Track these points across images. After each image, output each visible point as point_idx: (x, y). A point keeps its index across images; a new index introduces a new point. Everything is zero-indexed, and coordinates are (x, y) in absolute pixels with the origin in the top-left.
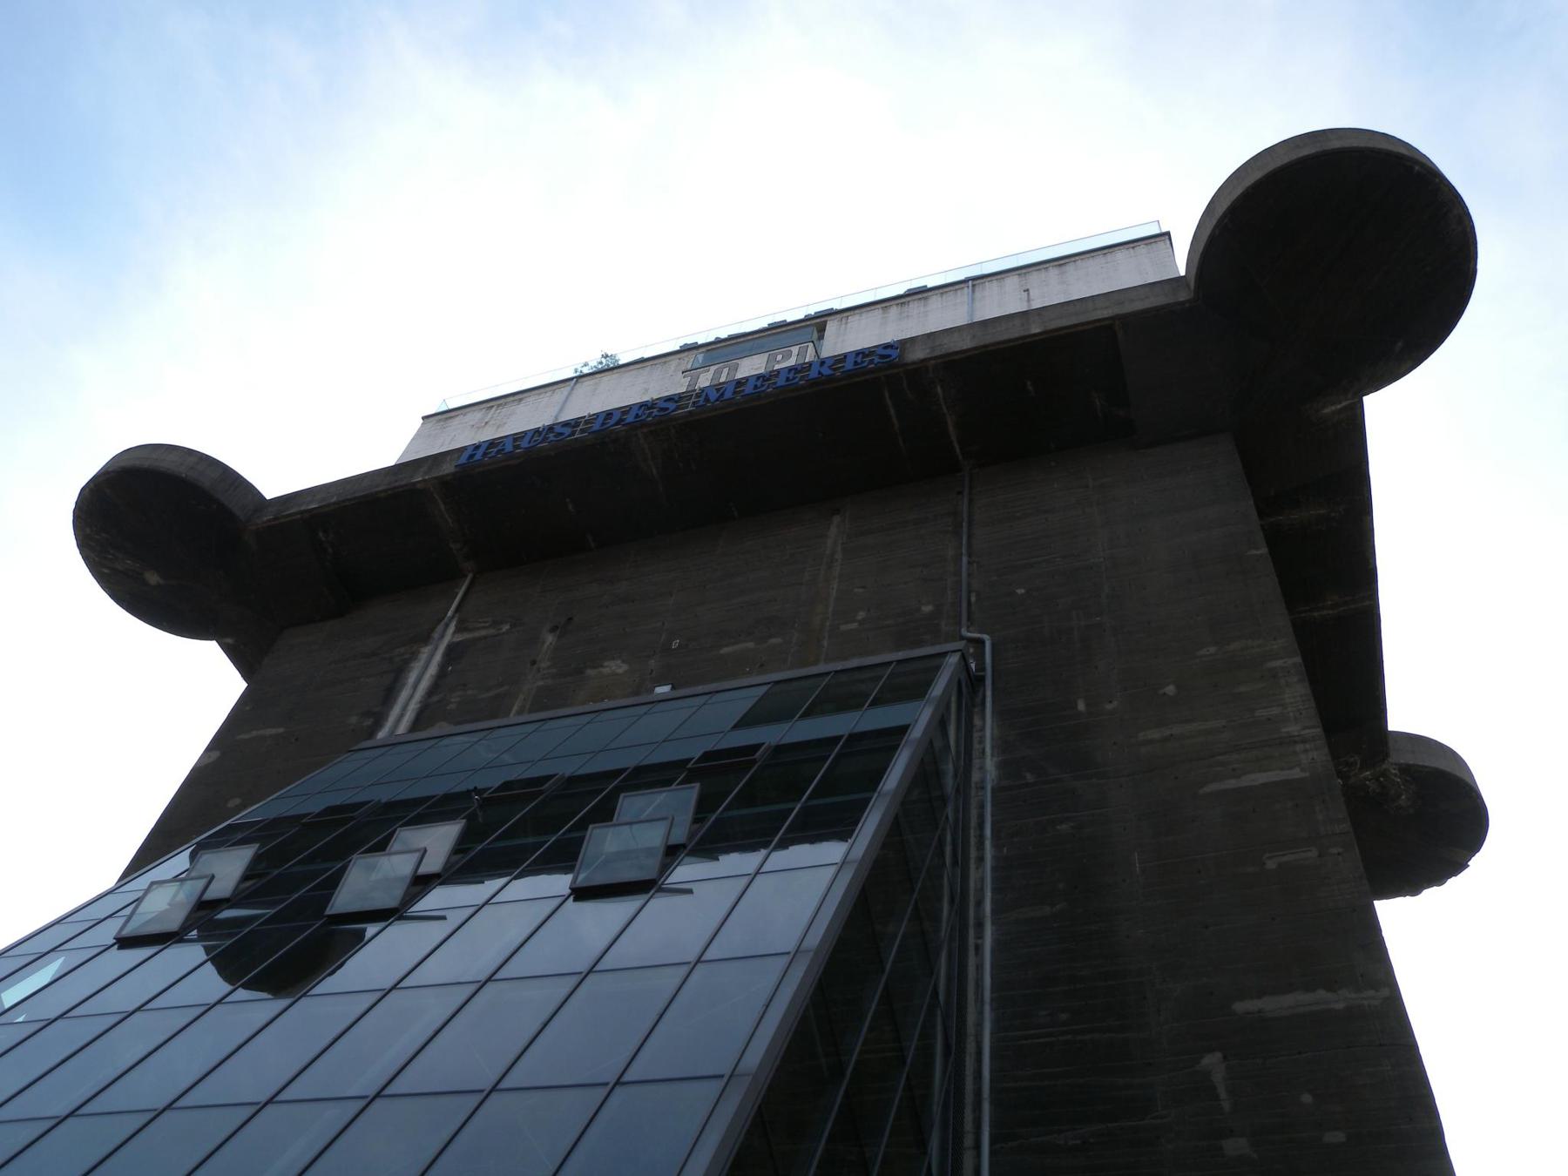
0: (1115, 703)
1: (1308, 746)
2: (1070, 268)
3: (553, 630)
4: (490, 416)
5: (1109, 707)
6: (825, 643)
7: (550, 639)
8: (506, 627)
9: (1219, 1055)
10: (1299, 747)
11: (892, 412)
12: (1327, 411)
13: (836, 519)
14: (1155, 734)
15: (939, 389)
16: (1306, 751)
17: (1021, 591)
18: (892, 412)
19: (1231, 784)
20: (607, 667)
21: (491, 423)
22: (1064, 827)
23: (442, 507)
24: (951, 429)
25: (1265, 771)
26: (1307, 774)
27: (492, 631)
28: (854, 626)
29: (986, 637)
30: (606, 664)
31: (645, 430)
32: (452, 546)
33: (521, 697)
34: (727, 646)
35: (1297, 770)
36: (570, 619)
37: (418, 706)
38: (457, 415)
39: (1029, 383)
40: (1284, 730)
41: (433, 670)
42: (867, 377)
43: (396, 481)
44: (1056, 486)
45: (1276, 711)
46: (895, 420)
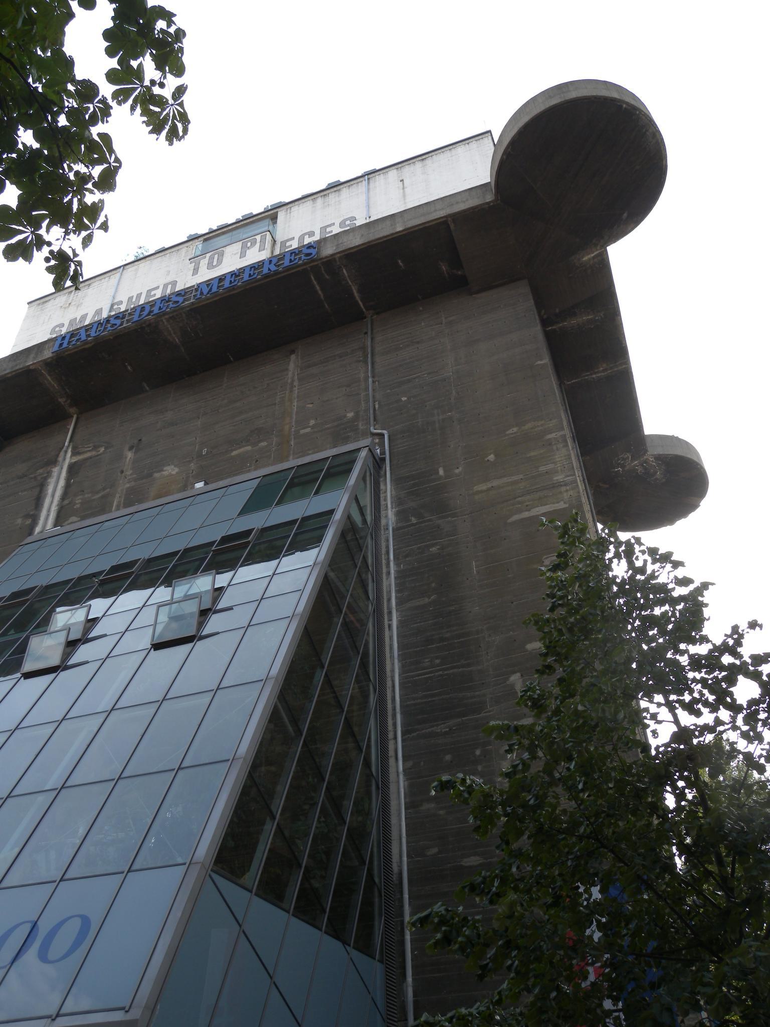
0: (460, 469)
1: (568, 488)
2: (429, 162)
3: (131, 449)
4: (71, 299)
5: (457, 471)
6: (292, 443)
7: (130, 455)
8: (102, 450)
9: (518, 674)
10: (563, 489)
11: (318, 288)
12: (585, 258)
13: (293, 357)
14: (483, 487)
15: (345, 271)
16: (567, 491)
17: (404, 399)
18: (318, 288)
19: (526, 515)
20: (165, 470)
21: (72, 304)
22: (434, 549)
23: (49, 378)
24: (356, 294)
25: (544, 505)
26: (567, 506)
27: (94, 453)
28: (308, 430)
29: (385, 432)
30: (165, 469)
31: (167, 317)
32: (60, 400)
33: (118, 495)
34: (235, 450)
35: (562, 503)
36: (140, 440)
37: (57, 508)
38: (50, 300)
39: (399, 261)
40: (555, 479)
41: (62, 483)
42: (299, 269)
43: (16, 365)
44: (423, 324)
45: (551, 466)
46: (320, 292)
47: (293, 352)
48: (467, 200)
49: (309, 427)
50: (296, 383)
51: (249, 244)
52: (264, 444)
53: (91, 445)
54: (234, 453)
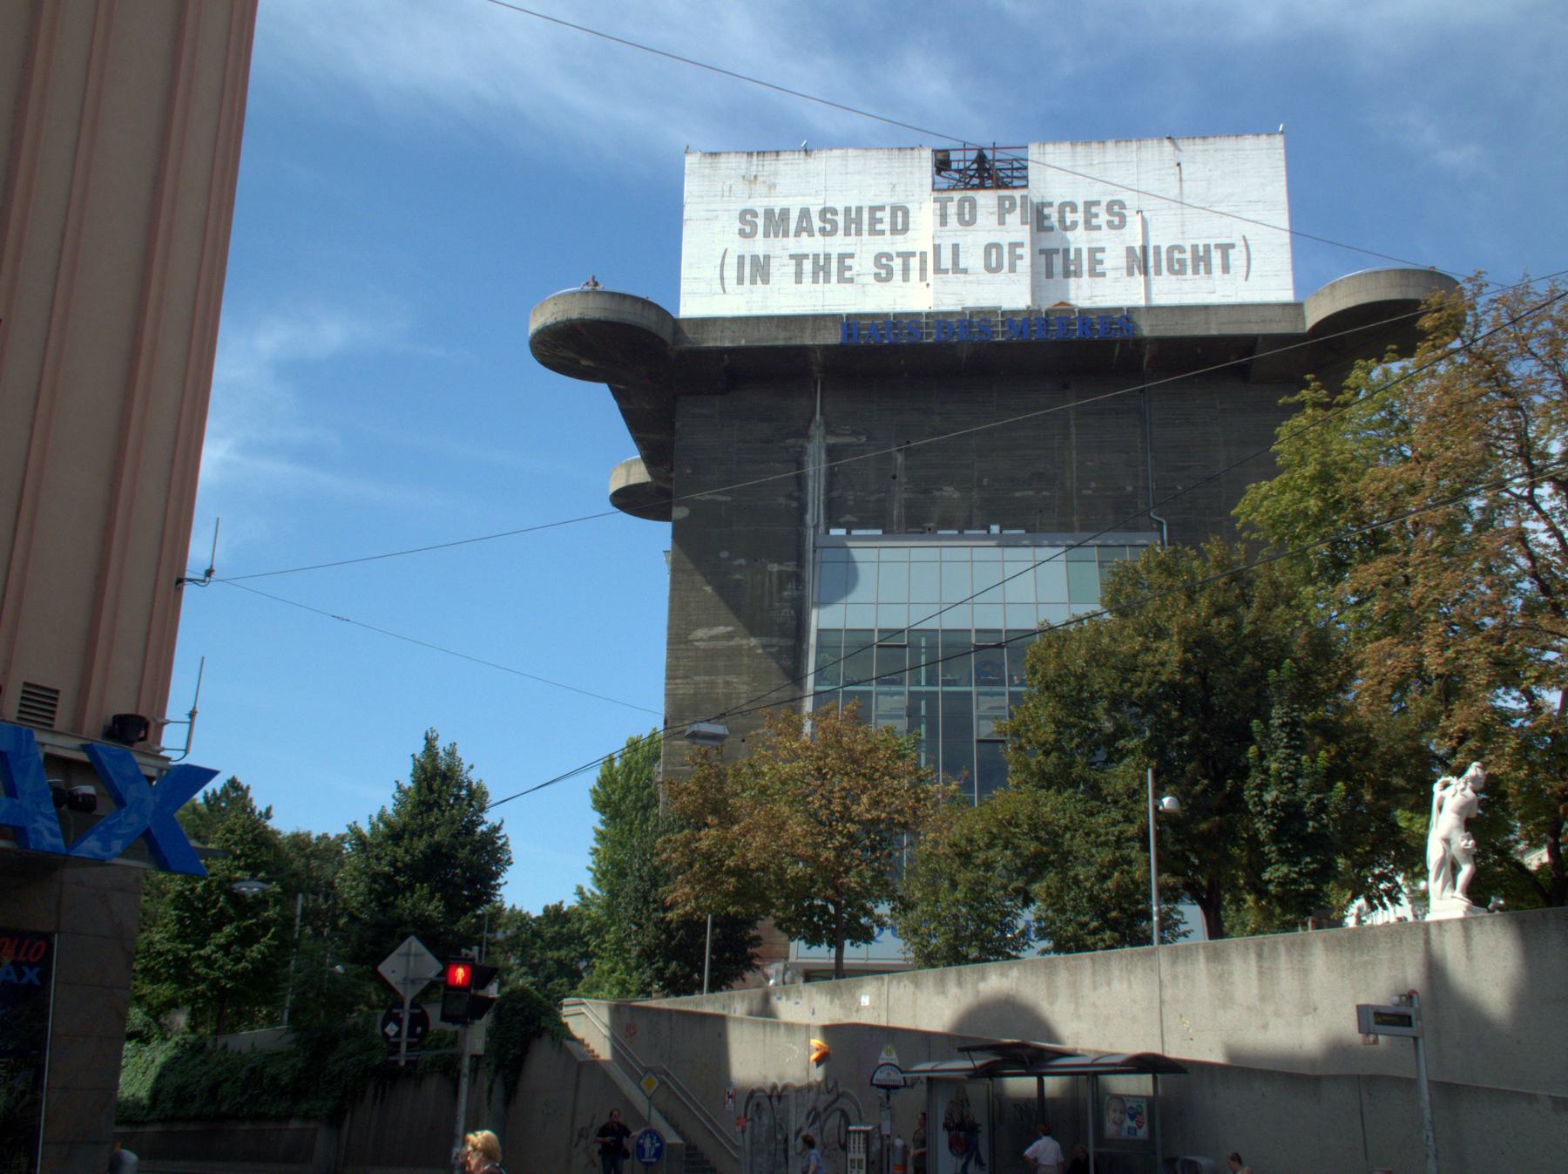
6: (1075, 501)
21: (760, 179)
28: (1089, 492)
29: (1164, 522)
30: (945, 488)
33: (896, 505)
43: (790, 339)
47: (1066, 387)
48: (1280, 321)
49: (1089, 489)
50: (1073, 430)
51: (1007, 204)
53: (847, 427)
54: (1018, 494)
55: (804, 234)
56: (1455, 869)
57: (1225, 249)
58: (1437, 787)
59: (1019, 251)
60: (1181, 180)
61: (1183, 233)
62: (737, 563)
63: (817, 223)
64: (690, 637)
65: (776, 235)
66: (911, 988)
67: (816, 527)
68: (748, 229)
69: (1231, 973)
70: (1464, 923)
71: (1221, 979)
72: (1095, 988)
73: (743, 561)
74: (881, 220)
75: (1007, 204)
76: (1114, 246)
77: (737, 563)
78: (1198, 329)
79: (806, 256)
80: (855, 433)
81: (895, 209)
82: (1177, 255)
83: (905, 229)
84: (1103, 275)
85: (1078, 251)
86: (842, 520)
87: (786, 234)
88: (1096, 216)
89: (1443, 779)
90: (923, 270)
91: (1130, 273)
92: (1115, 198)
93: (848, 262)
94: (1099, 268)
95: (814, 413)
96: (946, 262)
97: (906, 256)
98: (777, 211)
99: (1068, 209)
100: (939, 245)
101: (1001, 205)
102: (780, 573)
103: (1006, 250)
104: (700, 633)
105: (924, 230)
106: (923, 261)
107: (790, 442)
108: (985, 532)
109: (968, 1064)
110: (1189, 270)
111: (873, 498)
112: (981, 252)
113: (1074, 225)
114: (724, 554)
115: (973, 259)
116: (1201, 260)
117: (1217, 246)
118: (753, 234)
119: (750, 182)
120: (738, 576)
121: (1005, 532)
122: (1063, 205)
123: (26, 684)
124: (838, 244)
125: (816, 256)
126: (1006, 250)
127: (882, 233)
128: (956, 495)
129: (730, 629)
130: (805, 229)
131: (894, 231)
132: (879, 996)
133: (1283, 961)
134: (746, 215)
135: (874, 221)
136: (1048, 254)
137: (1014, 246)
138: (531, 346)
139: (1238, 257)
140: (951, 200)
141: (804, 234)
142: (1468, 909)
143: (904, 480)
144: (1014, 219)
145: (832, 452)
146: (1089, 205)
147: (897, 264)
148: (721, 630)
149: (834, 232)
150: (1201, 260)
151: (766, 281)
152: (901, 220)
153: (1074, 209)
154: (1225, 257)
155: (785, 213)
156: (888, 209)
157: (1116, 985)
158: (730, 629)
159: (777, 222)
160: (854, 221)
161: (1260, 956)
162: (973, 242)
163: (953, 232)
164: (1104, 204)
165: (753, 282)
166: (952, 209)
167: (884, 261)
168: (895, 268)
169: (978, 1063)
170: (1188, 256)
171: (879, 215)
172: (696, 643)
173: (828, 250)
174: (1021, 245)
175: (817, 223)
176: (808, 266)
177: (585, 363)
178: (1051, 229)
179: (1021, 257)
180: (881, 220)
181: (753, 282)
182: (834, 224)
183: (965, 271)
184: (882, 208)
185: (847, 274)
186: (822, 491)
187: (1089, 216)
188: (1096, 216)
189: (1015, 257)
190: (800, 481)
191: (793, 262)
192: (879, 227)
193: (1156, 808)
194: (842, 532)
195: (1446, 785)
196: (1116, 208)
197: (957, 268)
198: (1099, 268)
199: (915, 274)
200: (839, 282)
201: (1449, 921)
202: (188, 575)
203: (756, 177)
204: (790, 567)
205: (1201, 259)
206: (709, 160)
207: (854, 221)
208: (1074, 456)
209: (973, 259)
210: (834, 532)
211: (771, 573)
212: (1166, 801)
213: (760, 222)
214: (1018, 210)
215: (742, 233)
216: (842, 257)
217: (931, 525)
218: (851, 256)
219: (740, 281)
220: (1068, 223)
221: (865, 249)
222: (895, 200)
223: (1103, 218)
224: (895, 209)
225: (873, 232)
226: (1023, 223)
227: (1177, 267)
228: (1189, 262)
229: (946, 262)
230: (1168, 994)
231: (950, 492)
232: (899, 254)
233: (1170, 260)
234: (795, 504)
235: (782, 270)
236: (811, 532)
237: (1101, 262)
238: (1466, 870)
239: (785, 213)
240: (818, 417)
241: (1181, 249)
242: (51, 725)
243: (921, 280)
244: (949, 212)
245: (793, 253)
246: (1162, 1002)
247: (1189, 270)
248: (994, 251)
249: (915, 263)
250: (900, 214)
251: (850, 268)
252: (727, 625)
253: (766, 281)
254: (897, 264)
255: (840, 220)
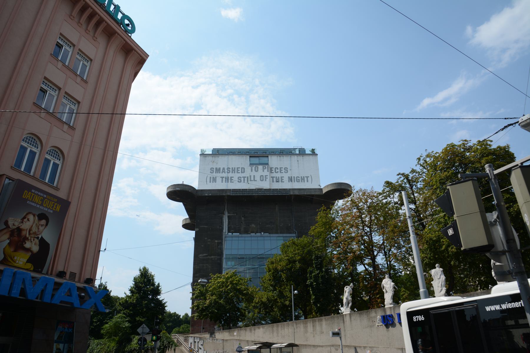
3: (243, 217)
7: (243, 218)
27: (233, 215)
28: (281, 226)
33: (242, 228)
41: (227, 220)
50: (278, 213)
51: (264, 168)
52: (273, 226)
55: (223, 173)
56: (349, 304)
57: (307, 177)
58: (345, 288)
59: (267, 177)
60: (298, 164)
61: (299, 174)
62: (209, 240)
63: (226, 171)
64: (199, 256)
65: (218, 173)
66: (245, 331)
67: (225, 232)
68: (212, 171)
69: (307, 326)
70: (350, 314)
71: (306, 327)
72: (281, 330)
73: (210, 240)
74: (239, 170)
75: (264, 168)
76: (286, 176)
77: (209, 240)
78: (302, 193)
79: (224, 177)
80: (233, 213)
81: (242, 168)
82: (298, 178)
83: (244, 172)
84: (284, 182)
85: (279, 177)
86: (231, 231)
87: (220, 173)
88: (282, 170)
89: (346, 286)
90: (248, 180)
91: (289, 182)
92: (285, 167)
93: (232, 178)
94: (283, 181)
95: (225, 209)
96: (252, 179)
97: (244, 177)
98: (218, 168)
99: (276, 169)
100: (251, 176)
101: (263, 168)
102: (218, 242)
103: (264, 177)
104: (201, 255)
105: (248, 172)
106: (248, 179)
107: (220, 215)
108: (260, 234)
109: (256, 347)
110: (300, 181)
111: (237, 227)
112: (259, 177)
113: (278, 172)
114: (206, 239)
115: (258, 178)
116: (303, 179)
117: (306, 177)
118: (213, 172)
119: (213, 162)
120: (209, 243)
121: (265, 234)
122: (275, 168)
123: (70, 272)
124: (230, 175)
125: (226, 177)
126: (264, 177)
127: (239, 173)
128: (255, 226)
129: (207, 254)
130: (223, 172)
131: (242, 172)
132: (238, 333)
133: (317, 323)
134: (212, 169)
135: (238, 170)
136: (273, 177)
137: (266, 176)
138: (167, 194)
139: (309, 179)
140: (253, 167)
141: (223, 173)
142: (351, 311)
143: (244, 223)
144: (266, 170)
145: (228, 217)
146: (281, 168)
147: (242, 179)
148: (205, 255)
149: (230, 172)
150: (303, 179)
151: (215, 182)
152: (243, 170)
153: (278, 169)
154: (307, 179)
155: (220, 168)
156: (240, 168)
157: (285, 329)
158: (207, 254)
159: (218, 170)
160: (233, 170)
161: (313, 323)
162: (258, 175)
163: (254, 173)
164: (284, 168)
165: (213, 182)
166: (253, 168)
167: (240, 178)
168: (242, 180)
169: (258, 346)
170: (300, 178)
171: (239, 169)
172: (200, 257)
173: (228, 176)
174: (267, 176)
175: (226, 171)
176: (224, 179)
177: (177, 198)
178: (273, 173)
179: (267, 178)
180: (239, 170)
181: (213, 182)
182: (230, 171)
183: (256, 181)
184: (239, 168)
185: (232, 181)
186: (227, 225)
187: (281, 170)
188: (282, 170)
189: (266, 178)
190: (222, 223)
191: (221, 178)
192: (239, 172)
193: (293, 293)
194: (231, 234)
195: (347, 288)
196: (286, 169)
197: (254, 180)
198: (283, 181)
199: (246, 181)
200: (231, 182)
201: (347, 314)
202: (101, 250)
203: (214, 161)
204: (220, 241)
205: (303, 179)
206: (204, 158)
207: (233, 170)
208: (278, 218)
209: (258, 178)
210: (229, 234)
211: (216, 242)
212: (296, 292)
213: (215, 170)
214: (267, 169)
215: (211, 172)
216: (231, 177)
217: (249, 232)
218: (233, 177)
219: (210, 182)
220: (277, 172)
221: (236, 176)
222: (243, 166)
223: (283, 171)
224: (242, 168)
225: (238, 172)
226: (268, 171)
227: (298, 181)
228: (300, 180)
229: (252, 179)
230: (295, 331)
231: (253, 225)
232: (243, 177)
233: (297, 179)
234: (221, 228)
235: (219, 180)
236: (224, 234)
237: (283, 179)
238: (350, 305)
239: (220, 168)
240: (226, 210)
241: (299, 177)
242: (75, 280)
243: (247, 182)
244: (253, 169)
245: (221, 176)
246: (294, 332)
247: (300, 181)
248: (262, 177)
249: (246, 179)
250: (243, 169)
251: (233, 180)
252: (206, 254)
253: (215, 182)
254: (242, 179)
255: (231, 170)
